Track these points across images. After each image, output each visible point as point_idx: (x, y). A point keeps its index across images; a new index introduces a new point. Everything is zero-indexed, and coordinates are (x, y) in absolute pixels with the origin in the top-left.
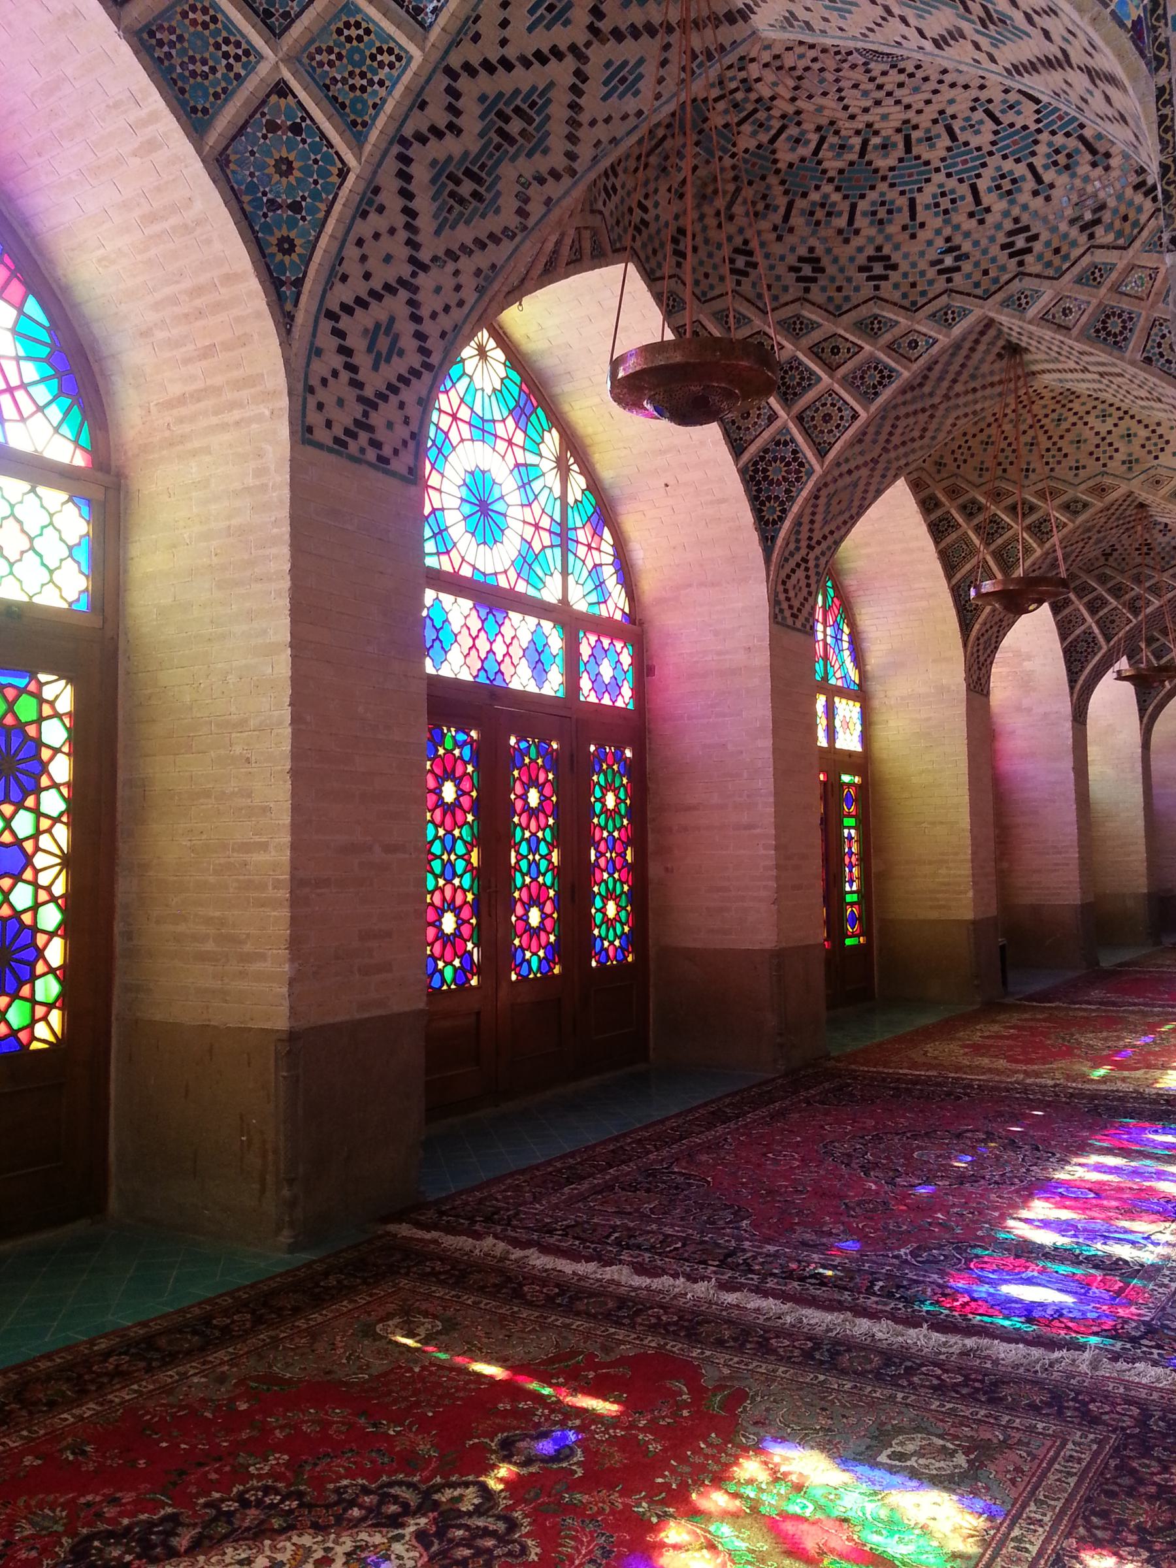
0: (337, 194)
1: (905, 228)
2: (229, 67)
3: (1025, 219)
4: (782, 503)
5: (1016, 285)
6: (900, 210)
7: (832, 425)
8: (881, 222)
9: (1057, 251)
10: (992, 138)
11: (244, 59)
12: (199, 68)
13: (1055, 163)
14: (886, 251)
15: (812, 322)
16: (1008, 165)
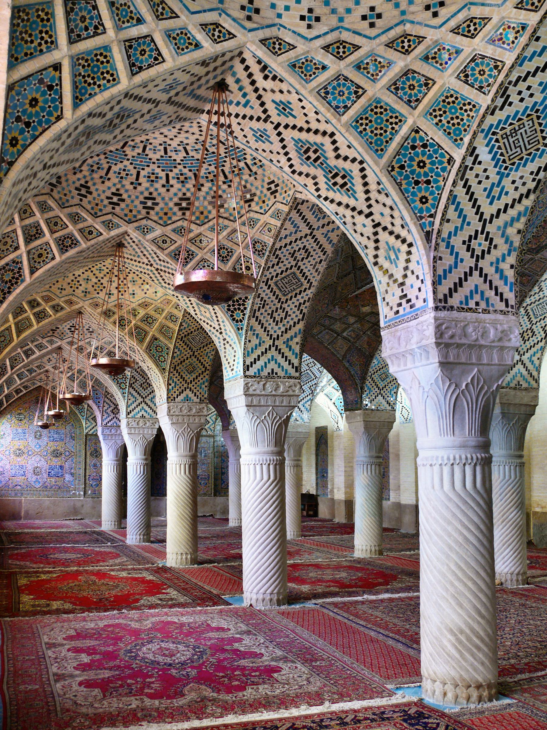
0: (50, 127)
1: (101, 177)
2: (40, 44)
3: (155, 195)
4: (5, 294)
5: (144, 222)
6: (103, 169)
7: (41, 260)
8: (93, 171)
9: (166, 214)
10: (159, 158)
11: (49, 44)
12: (26, 37)
13: (178, 178)
14: (89, 184)
15: (51, 207)
16: (158, 170)
